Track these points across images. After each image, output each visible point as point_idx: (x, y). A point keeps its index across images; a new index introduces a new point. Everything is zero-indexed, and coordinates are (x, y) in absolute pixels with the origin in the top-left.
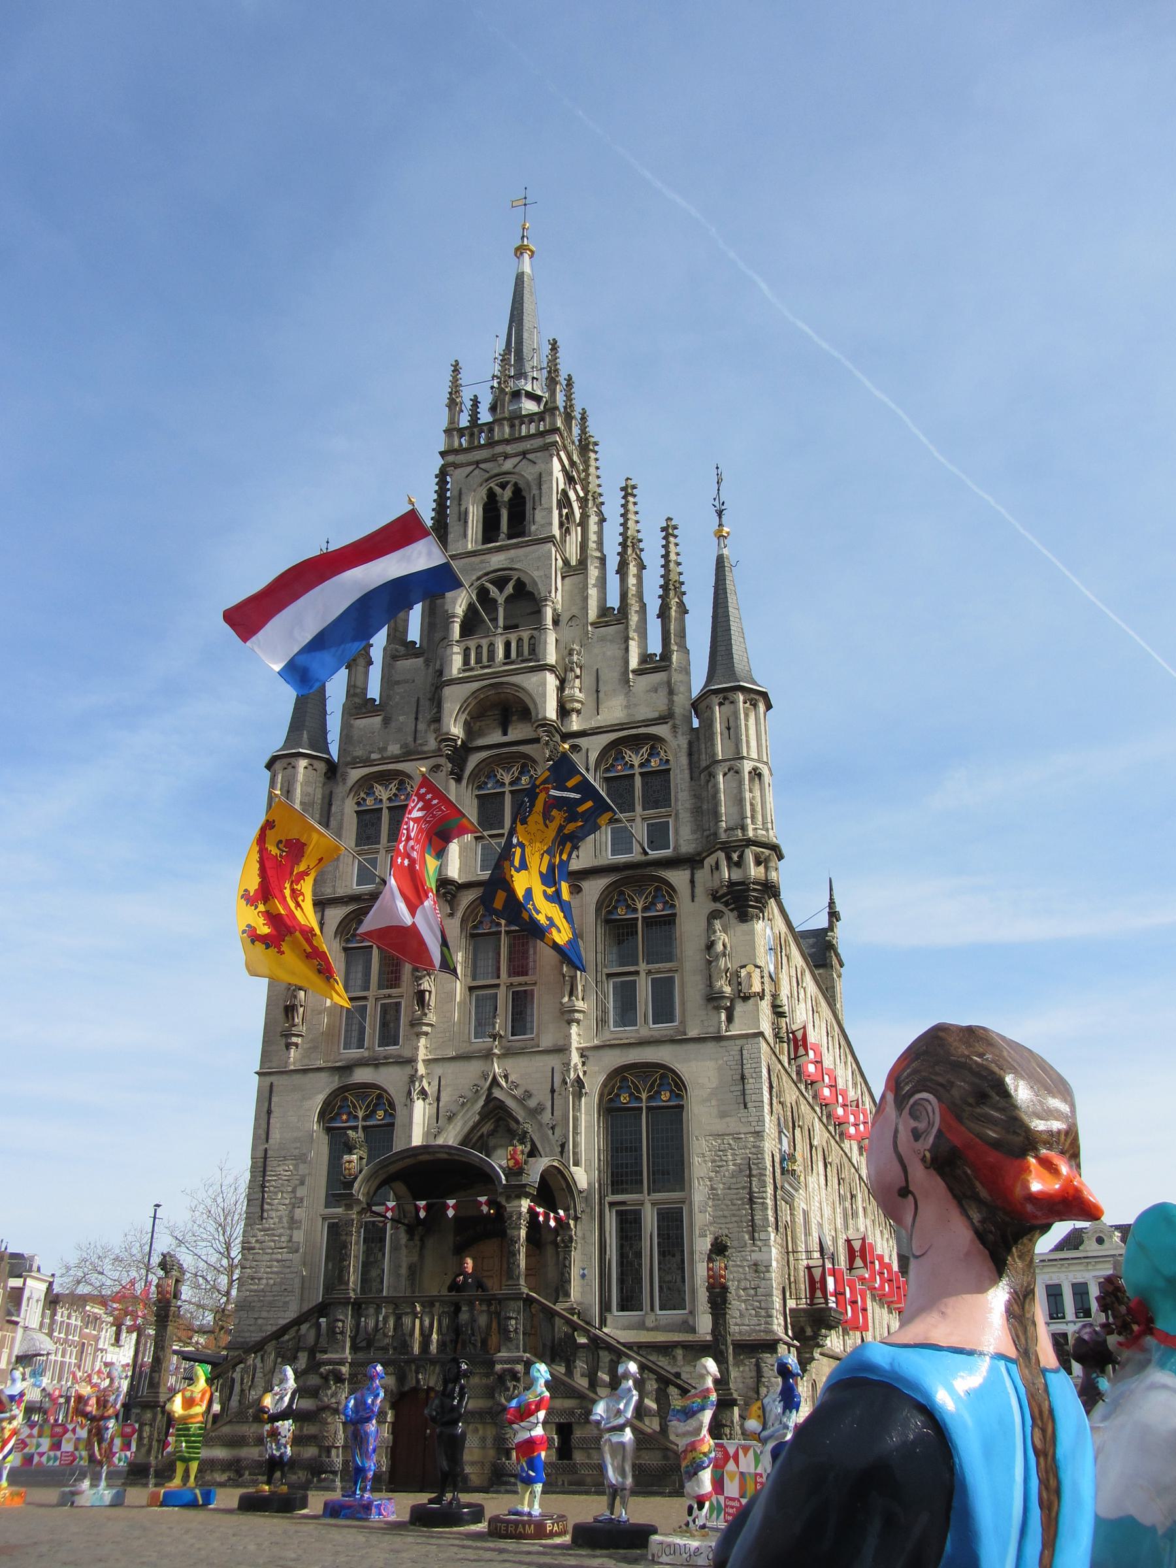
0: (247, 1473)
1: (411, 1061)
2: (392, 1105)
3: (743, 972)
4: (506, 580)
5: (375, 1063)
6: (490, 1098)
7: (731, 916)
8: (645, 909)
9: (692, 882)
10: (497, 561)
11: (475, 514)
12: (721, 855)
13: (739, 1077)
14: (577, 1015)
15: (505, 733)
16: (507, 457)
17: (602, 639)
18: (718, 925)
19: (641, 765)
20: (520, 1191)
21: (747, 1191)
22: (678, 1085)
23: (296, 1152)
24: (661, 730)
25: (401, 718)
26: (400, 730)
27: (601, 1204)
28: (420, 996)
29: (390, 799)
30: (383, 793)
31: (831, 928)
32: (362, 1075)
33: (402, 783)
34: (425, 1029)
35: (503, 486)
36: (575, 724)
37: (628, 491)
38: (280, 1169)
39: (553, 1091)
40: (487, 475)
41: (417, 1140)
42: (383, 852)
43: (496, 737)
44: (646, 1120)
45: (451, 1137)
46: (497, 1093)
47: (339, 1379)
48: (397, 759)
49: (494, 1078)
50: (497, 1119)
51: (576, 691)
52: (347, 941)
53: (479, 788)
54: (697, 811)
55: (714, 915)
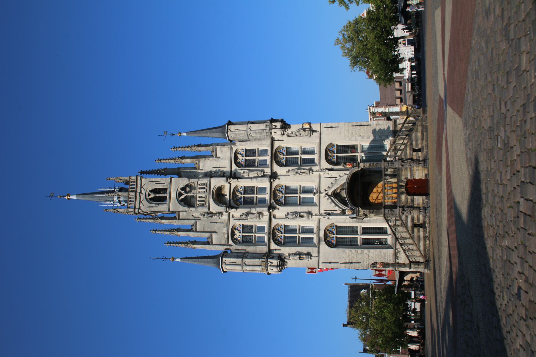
4: (180, 193)
5: (319, 230)
9: (278, 140)
10: (173, 195)
12: (273, 131)
15: (226, 195)
16: (141, 192)
17: (204, 167)
22: (331, 145)
25: (215, 228)
26: (219, 228)
30: (238, 235)
32: (322, 235)
33: (235, 229)
35: (149, 195)
36: (229, 174)
43: (228, 197)
46: (330, 194)
48: (228, 228)
49: (326, 194)
50: (336, 195)
54: (259, 140)
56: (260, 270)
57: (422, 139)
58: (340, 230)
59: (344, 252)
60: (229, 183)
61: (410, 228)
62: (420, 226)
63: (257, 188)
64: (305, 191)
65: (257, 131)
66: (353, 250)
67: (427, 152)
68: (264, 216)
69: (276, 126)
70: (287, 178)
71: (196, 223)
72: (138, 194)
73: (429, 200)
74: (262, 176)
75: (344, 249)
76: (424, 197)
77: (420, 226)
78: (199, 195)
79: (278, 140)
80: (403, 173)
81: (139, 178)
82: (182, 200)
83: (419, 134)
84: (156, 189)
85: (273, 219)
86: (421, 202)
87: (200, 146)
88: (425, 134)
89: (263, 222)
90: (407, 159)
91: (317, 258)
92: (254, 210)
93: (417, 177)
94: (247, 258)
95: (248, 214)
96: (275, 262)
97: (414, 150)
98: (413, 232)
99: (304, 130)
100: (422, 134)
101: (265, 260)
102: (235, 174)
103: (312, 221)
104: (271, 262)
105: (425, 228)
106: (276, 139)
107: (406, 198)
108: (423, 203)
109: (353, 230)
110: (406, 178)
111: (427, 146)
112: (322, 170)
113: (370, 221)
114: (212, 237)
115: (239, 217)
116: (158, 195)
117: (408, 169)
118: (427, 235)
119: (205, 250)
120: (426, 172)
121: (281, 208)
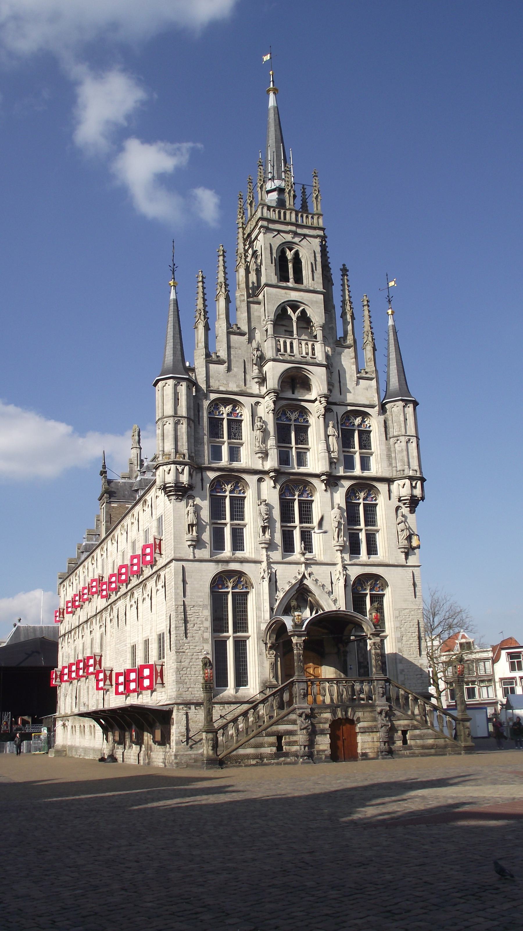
0: (265, 759)
5: (242, 561)
9: (389, 491)
10: (294, 296)
12: (407, 481)
13: (412, 584)
15: (293, 393)
16: (296, 234)
21: (417, 634)
23: (201, 603)
26: (235, 376)
32: (233, 566)
33: (234, 407)
37: (344, 271)
38: (192, 611)
39: (332, 583)
40: (284, 241)
46: (305, 582)
56: (167, 450)
57: (424, 747)
58: (241, 601)
59: (204, 606)
60: (316, 400)
61: (275, 728)
62: (280, 748)
63: (308, 449)
64: (306, 537)
65: (405, 453)
66: (208, 624)
67: (403, 756)
68: (260, 461)
69: (415, 487)
70: (327, 505)
71: (243, 334)
72: (293, 228)
73: (325, 762)
74: (330, 459)
75: (209, 607)
76: (329, 752)
78: (295, 343)
79: (389, 491)
80: (366, 714)
81: (321, 233)
82: (284, 310)
83: (431, 741)
84: (300, 262)
85: (256, 477)
86: (321, 747)
87: (374, 349)
88: (433, 751)
89: (247, 458)
90: (391, 721)
91: (191, 557)
92: (272, 442)
94: (189, 425)
95: (265, 432)
96: (185, 478)
98: (268, 735)
99: (409, 538)
100: (432, 747)
101: (187, 460)
103: (256, 549)
104: (183, 470)
106: (391, 486)
107: (327, 719)
108: (319, 751)
109: (241, 624)
110: (358, 718)
111: (413, 755)
112: (344, 568)
113: (260, 654)
114: (220, 362)
115: (259, 415)
116: (290, 265)
117: (375, 723)
118: (265, 760)
119: (193, 347)
120: (371, 755)
121: (276, 493)
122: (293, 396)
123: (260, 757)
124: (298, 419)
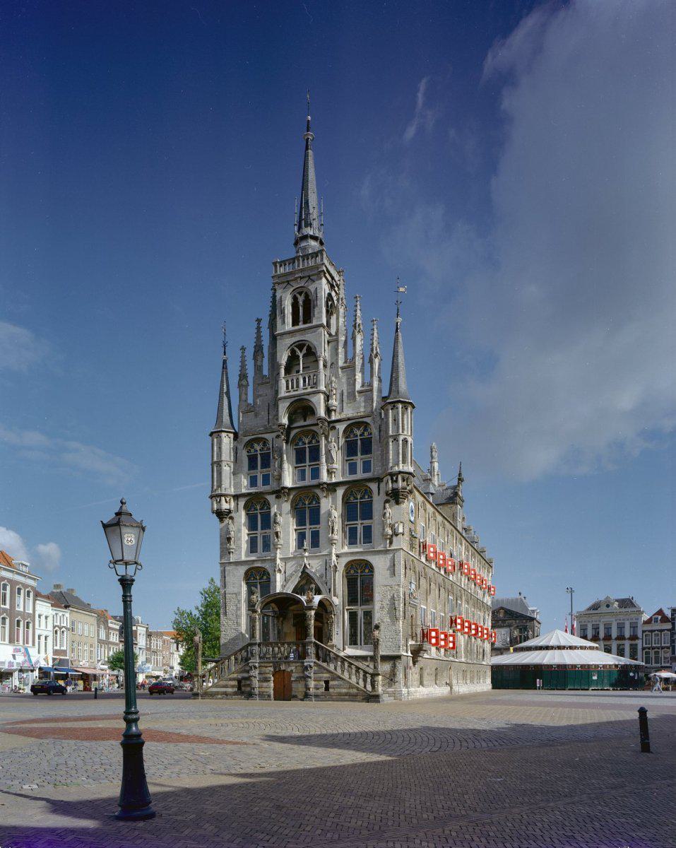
1: (274, 560)
2: (269, 575)
3: (396, 525)
6: (303, 572)
7: (393, 502)
8: (361, 498)
9: (379, 488)
11: (288, 310)
14: (334, 541)
15: (305, 420)
18: (387, 505)
19: (361, 435)
20: (311, 608)
24: (368, 420)
27: (343, 609)
28: (277, 533)
29: (260, 450)
30: (257, 447)
31: (458, 485)
33: (265, 442)
34: (279, 546)
39: (326, 569)
41: (278, 591)
42: (259, 473)
43: (302, 423)
44: (360, 582)
45: (289, 590)
47: (255, 667)
51: (334, 402)
52: (249, 511)
53: (296, 445)
55: (387, 501)
57: (340, 694)
63: (318, 464)
74: (328, 471)
77: (239, 688)
85: (274, 496)
93: (294, 685)
97: (327, 682)
100: (346, 694)
102: (334, 428)
105: (235, 694)
108: (263, 692)
122: (305, 423)
123: (226, 694)
124: (311, 441)
